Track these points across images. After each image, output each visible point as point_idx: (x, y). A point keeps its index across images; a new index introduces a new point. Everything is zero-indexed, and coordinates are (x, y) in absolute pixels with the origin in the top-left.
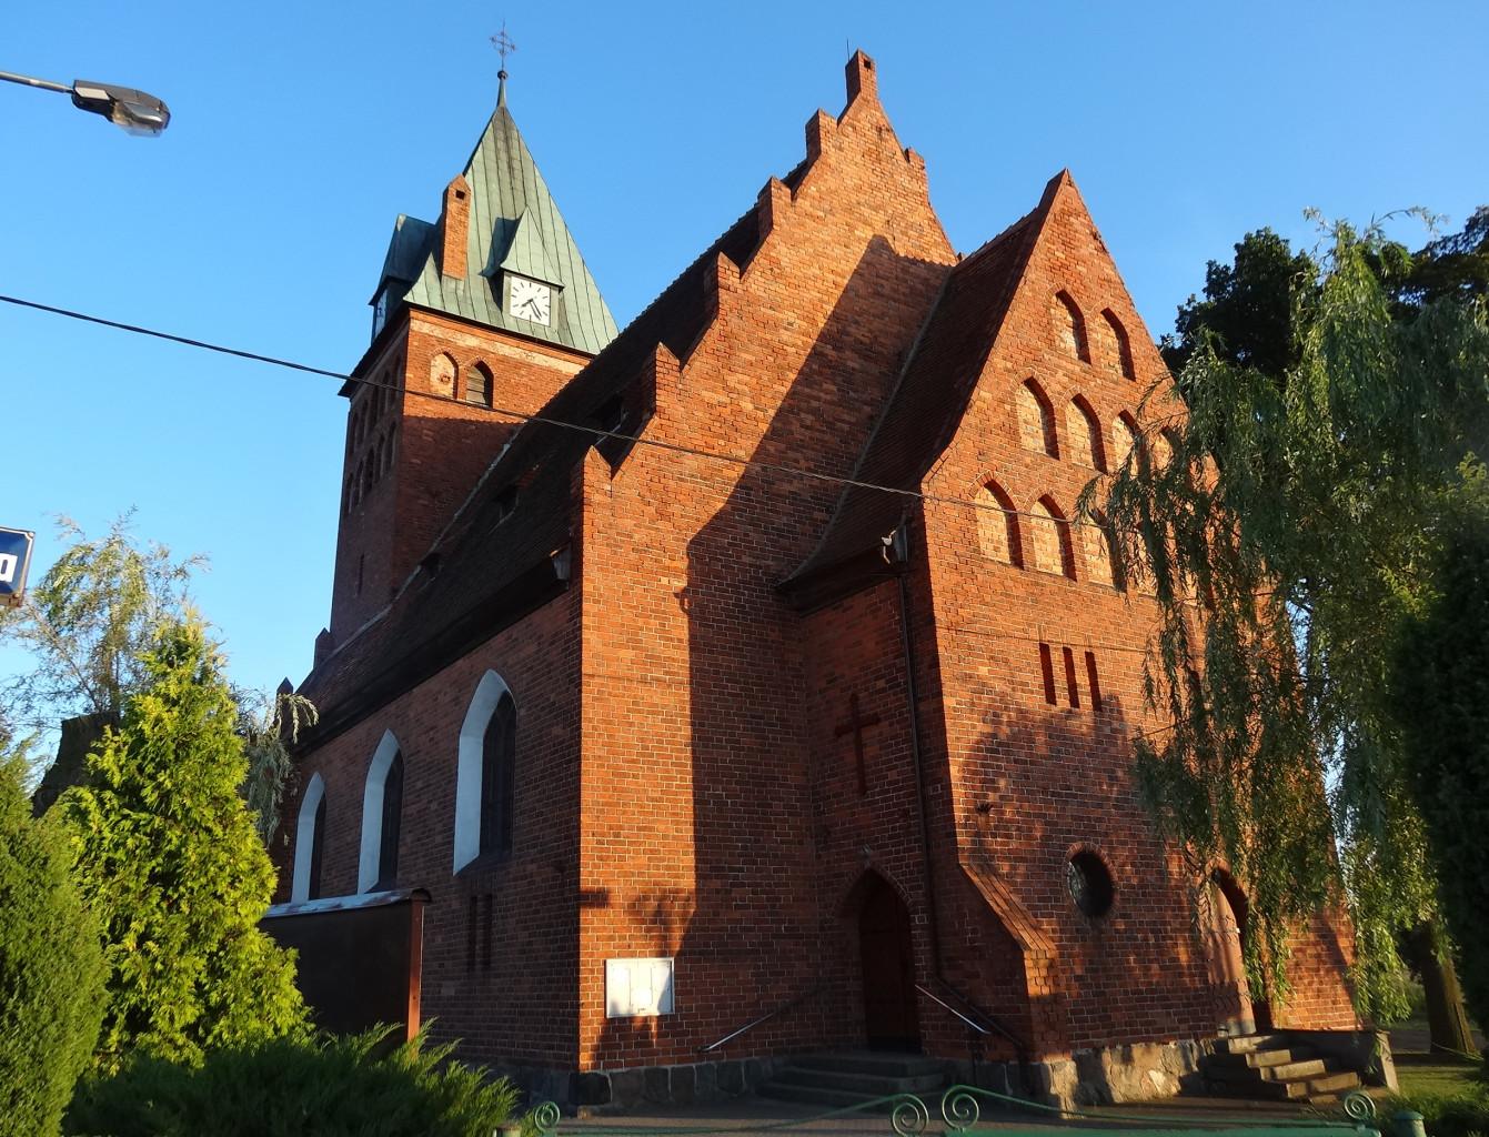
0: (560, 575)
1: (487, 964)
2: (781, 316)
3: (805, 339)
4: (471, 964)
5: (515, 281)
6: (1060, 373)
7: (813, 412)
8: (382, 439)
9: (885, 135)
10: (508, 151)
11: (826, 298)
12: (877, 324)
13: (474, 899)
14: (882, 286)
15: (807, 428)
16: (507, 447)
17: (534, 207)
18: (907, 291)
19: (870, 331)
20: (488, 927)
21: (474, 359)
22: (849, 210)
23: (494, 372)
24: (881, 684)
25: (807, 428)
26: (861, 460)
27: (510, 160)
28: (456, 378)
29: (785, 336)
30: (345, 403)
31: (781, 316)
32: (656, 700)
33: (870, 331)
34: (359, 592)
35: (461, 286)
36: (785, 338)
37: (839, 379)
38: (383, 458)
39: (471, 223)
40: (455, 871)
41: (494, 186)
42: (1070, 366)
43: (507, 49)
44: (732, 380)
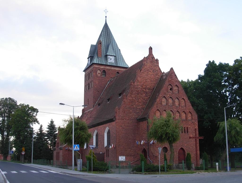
0: (114, 120)
1: (108, 156)
2: (138, 87)
3: (141, 89)
4: (107, 156)
5: (109, 56)
6: (168, 95)
7: (142, 98)
8: (90, 82)
9: (153, 58)
10: (107, 31)
11: (144, 83)
12: (151, 85)
13: (107, 150)
14: (152, 80)
15: (141, 100)
16: (108, 83)
17: (112, 43)
18: (155, 79)
19: (150, 86)
20: (108, 153)
21: (103, 70)
22: (148, 70)
23: (106, 71)
24: (146, 131)
25: (141, 100)
26: (148, 103)
27: (108, 32)
28: (101, 73)
29: (139, 89)
30: (84, 72)
31: (138, 87)
32: (124, 132)
33: (150, 86)
34: (88, 104)
35: (101, 58)
36: (139, 90)
37: (145, 93)
38: (91, 84)
39: (102, 48)
40: (105, 147)
41: (105, 39)
42: (170, 94)
43: (107, 12)
44: (132, 96)
